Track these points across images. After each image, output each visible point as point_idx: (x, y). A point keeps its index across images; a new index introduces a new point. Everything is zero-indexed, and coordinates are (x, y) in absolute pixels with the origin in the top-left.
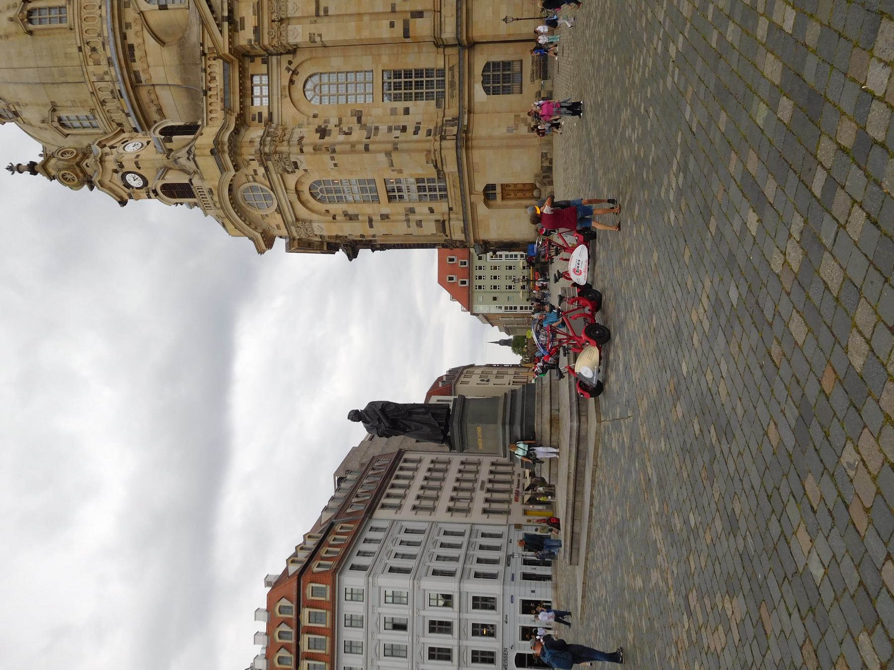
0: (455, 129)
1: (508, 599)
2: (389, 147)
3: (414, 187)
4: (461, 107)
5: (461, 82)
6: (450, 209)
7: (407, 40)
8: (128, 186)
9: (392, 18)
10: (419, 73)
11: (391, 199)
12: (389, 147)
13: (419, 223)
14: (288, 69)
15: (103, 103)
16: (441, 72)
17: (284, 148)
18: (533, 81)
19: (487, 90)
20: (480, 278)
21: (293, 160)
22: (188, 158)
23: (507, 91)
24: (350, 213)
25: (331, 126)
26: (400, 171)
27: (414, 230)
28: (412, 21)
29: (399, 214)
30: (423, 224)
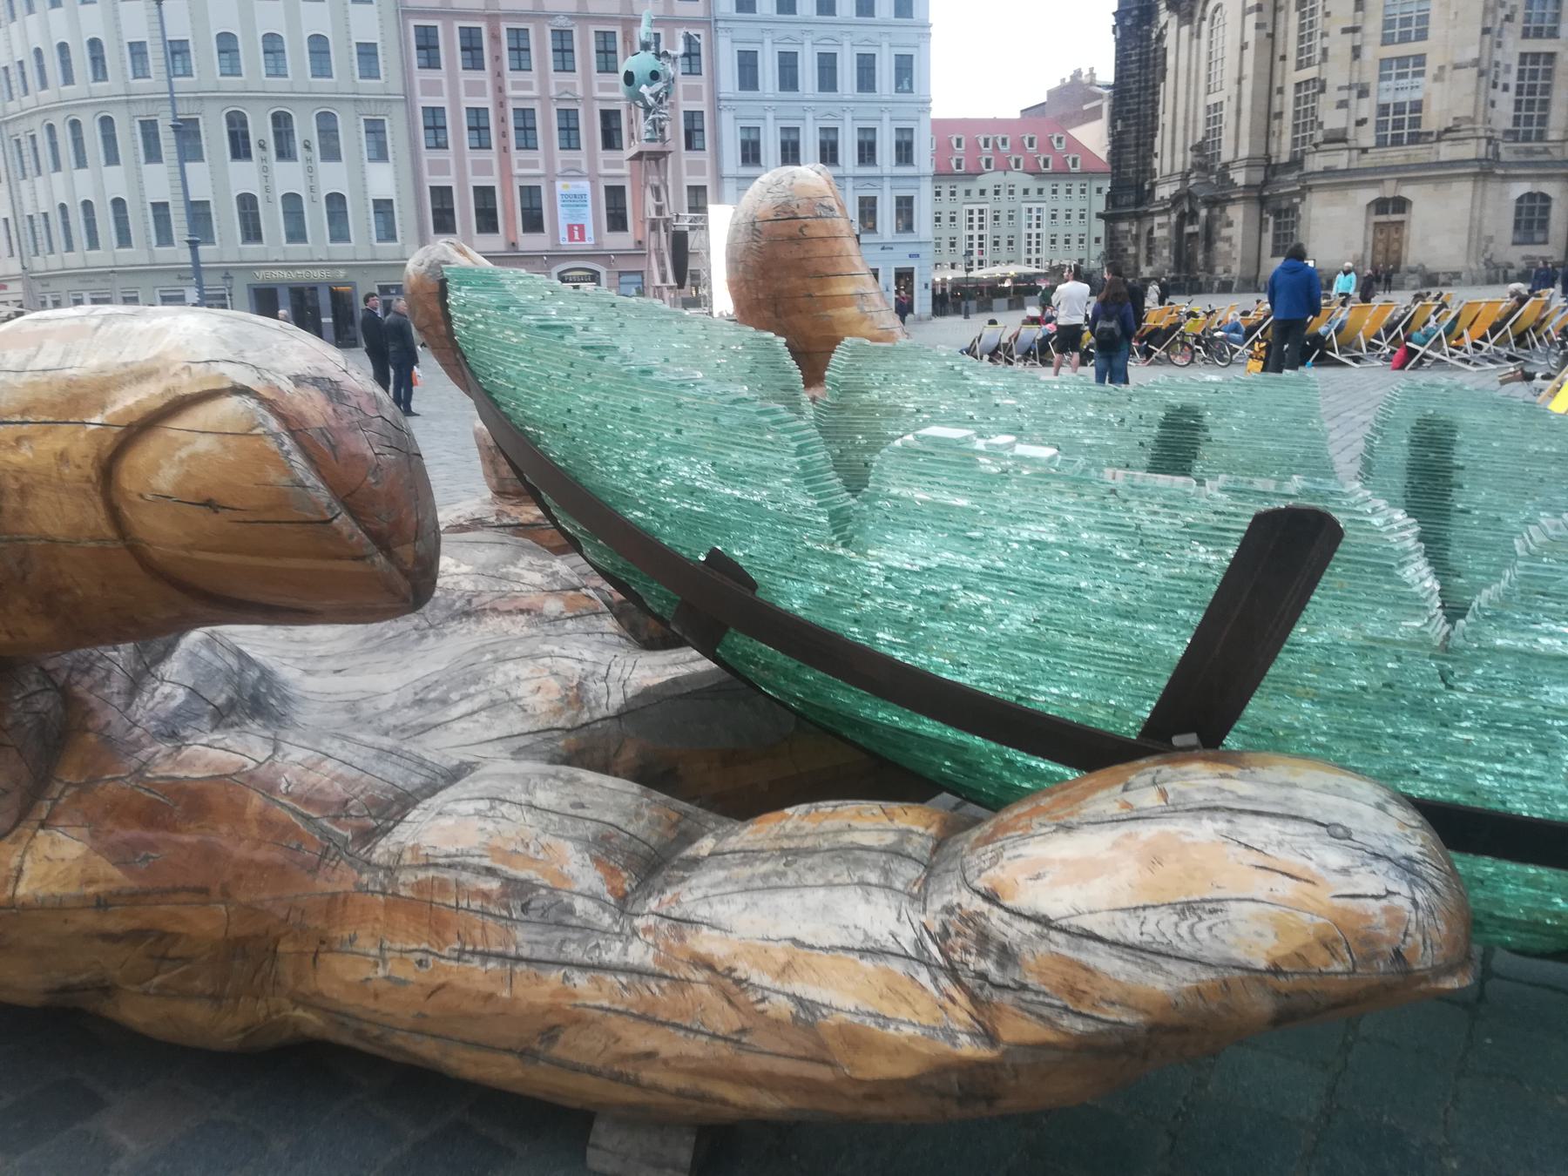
1: (914, 250)
2: (1485, 65)
3: (1403, 97)
4: (1508, 164)
5: (1536, 164)
6: (1364, 150)
10: (1545, 104)
11: (1385, 63)
12: (1485, 65)
13: (1343, 104)
16: (1541, 136)
18: (1524, 258)
19: (1520, 200)
26: (1437, 78)
29: (1360, 72)
30: (1344, 111)
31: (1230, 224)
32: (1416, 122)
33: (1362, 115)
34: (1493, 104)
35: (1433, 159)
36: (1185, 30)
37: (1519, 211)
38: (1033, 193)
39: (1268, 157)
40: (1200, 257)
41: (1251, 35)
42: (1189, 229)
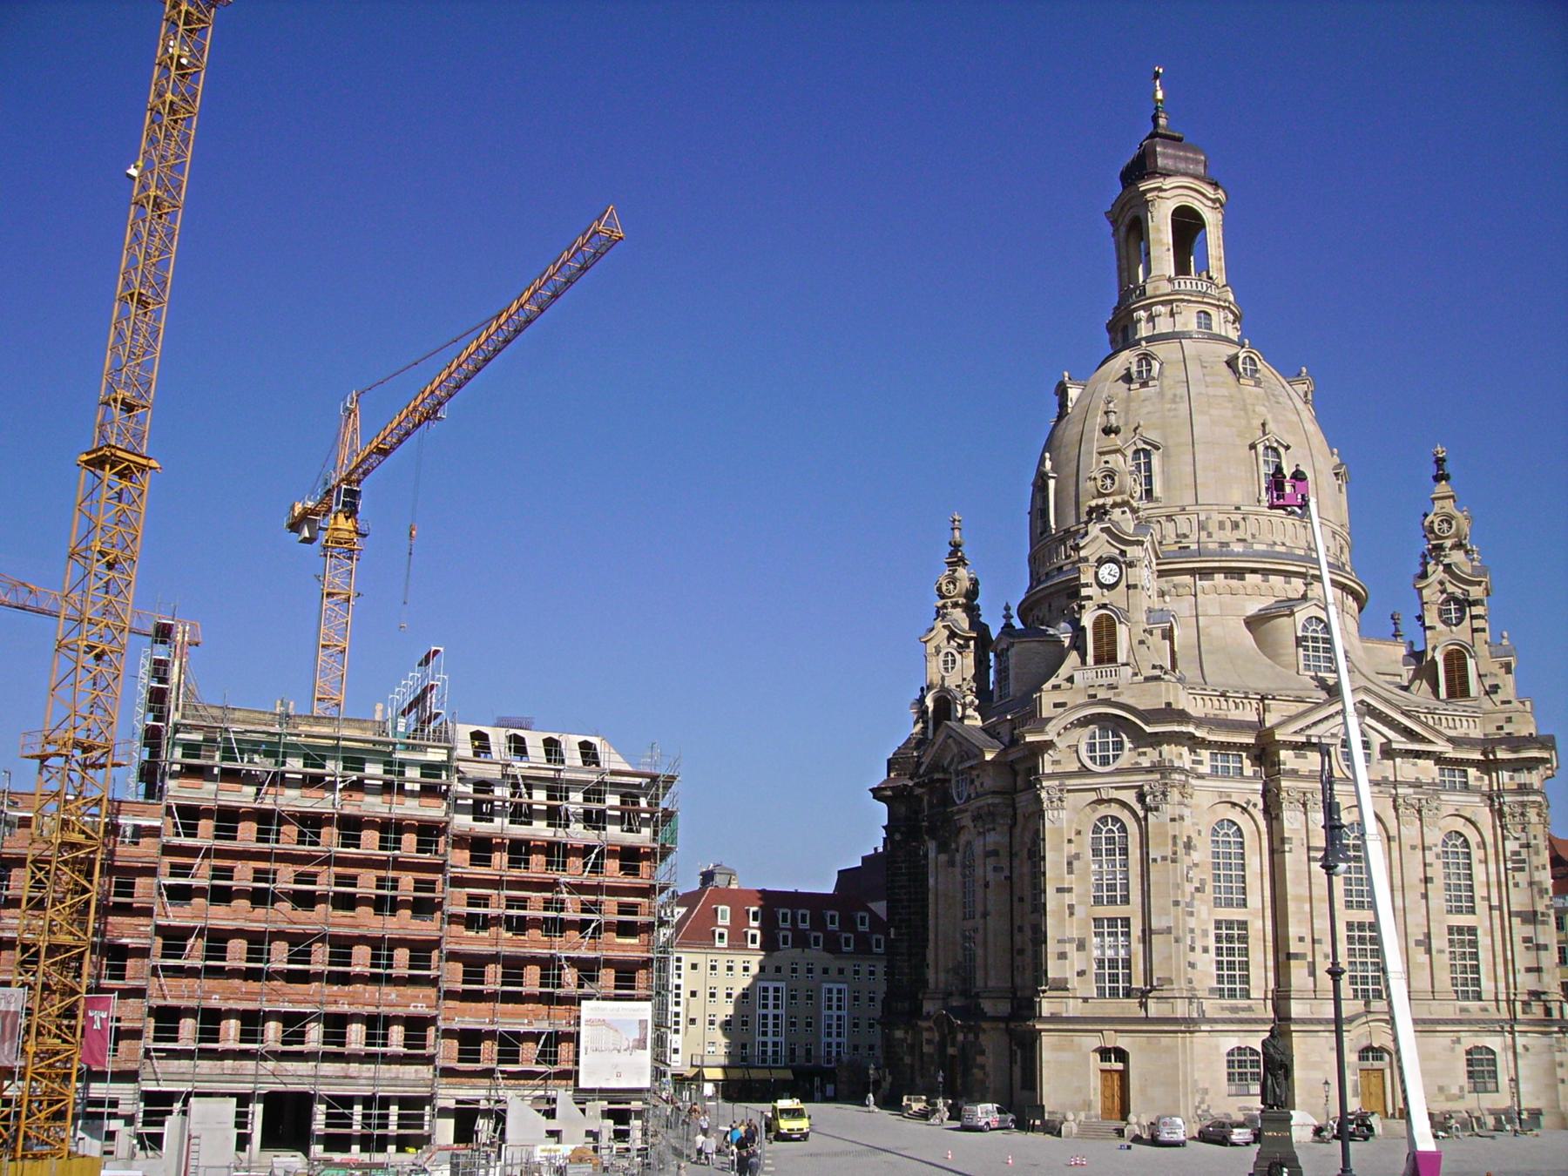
0: (1195, 1015)
6: (1085, 1000)
7: (1282, 957)
8: (1101, 562)
9: (1308, 939)
10: (1245, 966)
11: (1098, 922)
14: (1248, 803)
15: (1170, 518)
16: (1246, 994)
17: (1174, 795)
18: (1240, 1109)
19: (1231, 1053)
20: (730, 968)
21: (1163, 807)
22: (1154, 667)
23: (1230, 1076)
24: (1076, 863)
25: (1196, 856)
27: (1052, 947)
28: (1304, 963)
31: (983, 1053)
32: (1128, 978)
33: (1077, 968)
34: (1192, 965)
35: (1143, 1014)
36: (943, 858)
37: (1230, 1064)
38: (833, 972)
39: (1014, 994)
40: (959, 1081)
41: (991, 876)
42: (951, 1051)
